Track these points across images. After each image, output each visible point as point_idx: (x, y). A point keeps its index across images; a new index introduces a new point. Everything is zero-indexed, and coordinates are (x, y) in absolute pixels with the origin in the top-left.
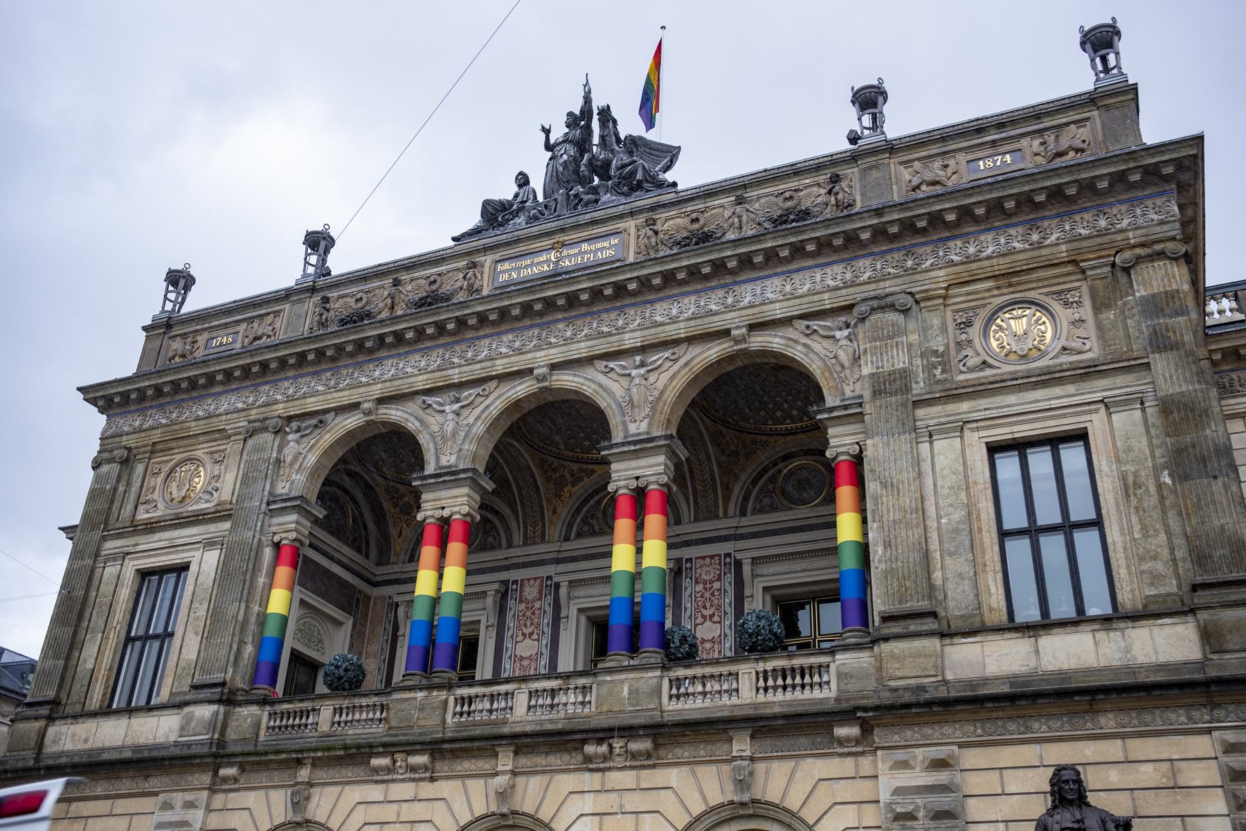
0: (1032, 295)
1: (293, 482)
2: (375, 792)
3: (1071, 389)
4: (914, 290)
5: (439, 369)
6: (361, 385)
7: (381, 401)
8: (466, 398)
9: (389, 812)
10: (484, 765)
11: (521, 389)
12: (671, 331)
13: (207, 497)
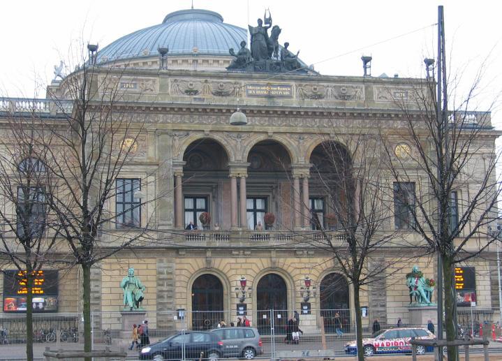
2: (233, 261)
6: (203, 124)
7: (211, 131)
9: (238, 266)
10: (267, 254)
12: (311, 130)
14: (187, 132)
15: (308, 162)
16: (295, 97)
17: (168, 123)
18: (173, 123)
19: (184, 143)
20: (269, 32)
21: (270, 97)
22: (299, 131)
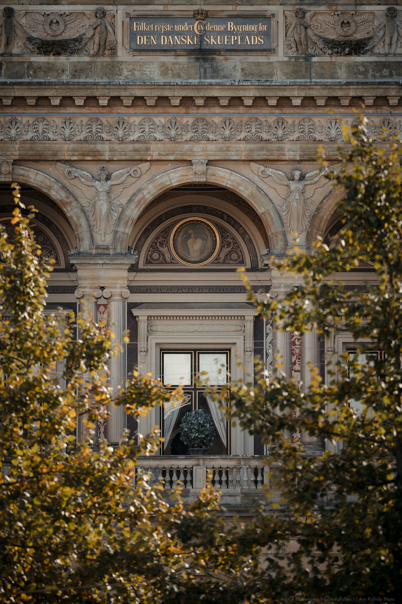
7: (15, 163)
8: (118, 177)
16: (281, 49)
22: (288, 155)
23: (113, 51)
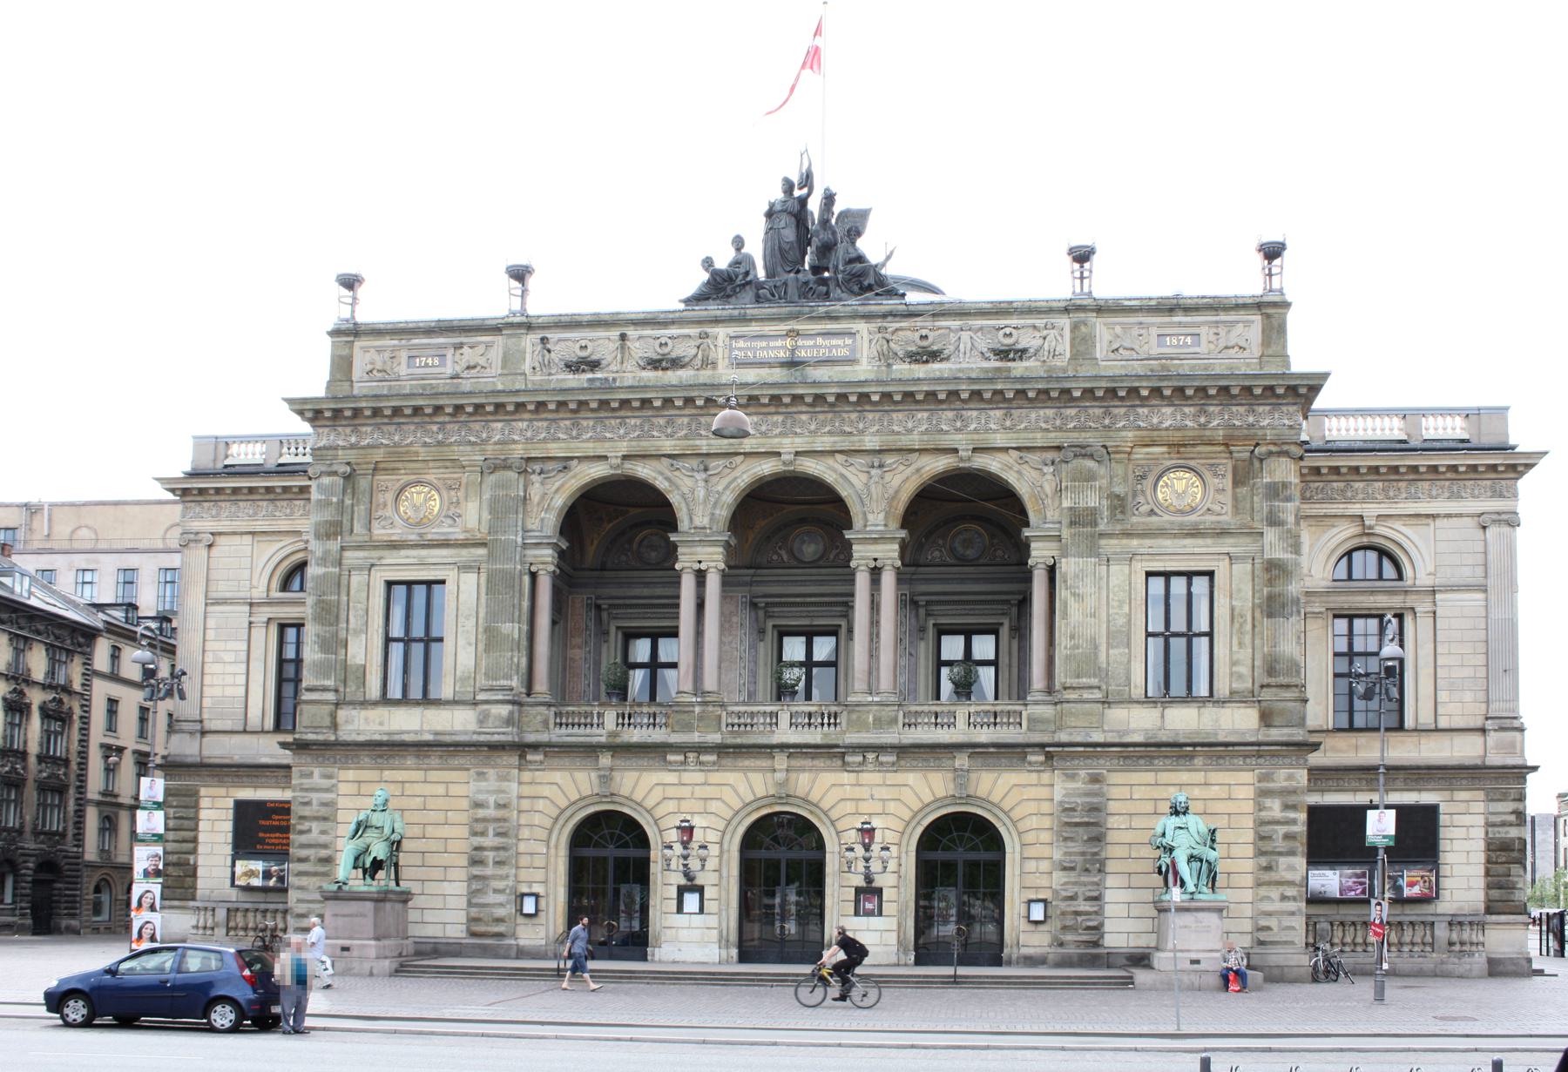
0: (1192, 463)
1: (542, 520)
3: (1209, 541)
4: (1108, 444)
5: (686, 437)
7: (625, 457)
8: (715, 467)
11: (767, 468)
12: (905, 441)
13: (450, 521)
14: (565, 463)
15: (894, 525)
17: (514, 442)
18: (528, 440)
19: (557, 491)
20: (814, 205)
21: (792, 364)
23: (714, 364)
